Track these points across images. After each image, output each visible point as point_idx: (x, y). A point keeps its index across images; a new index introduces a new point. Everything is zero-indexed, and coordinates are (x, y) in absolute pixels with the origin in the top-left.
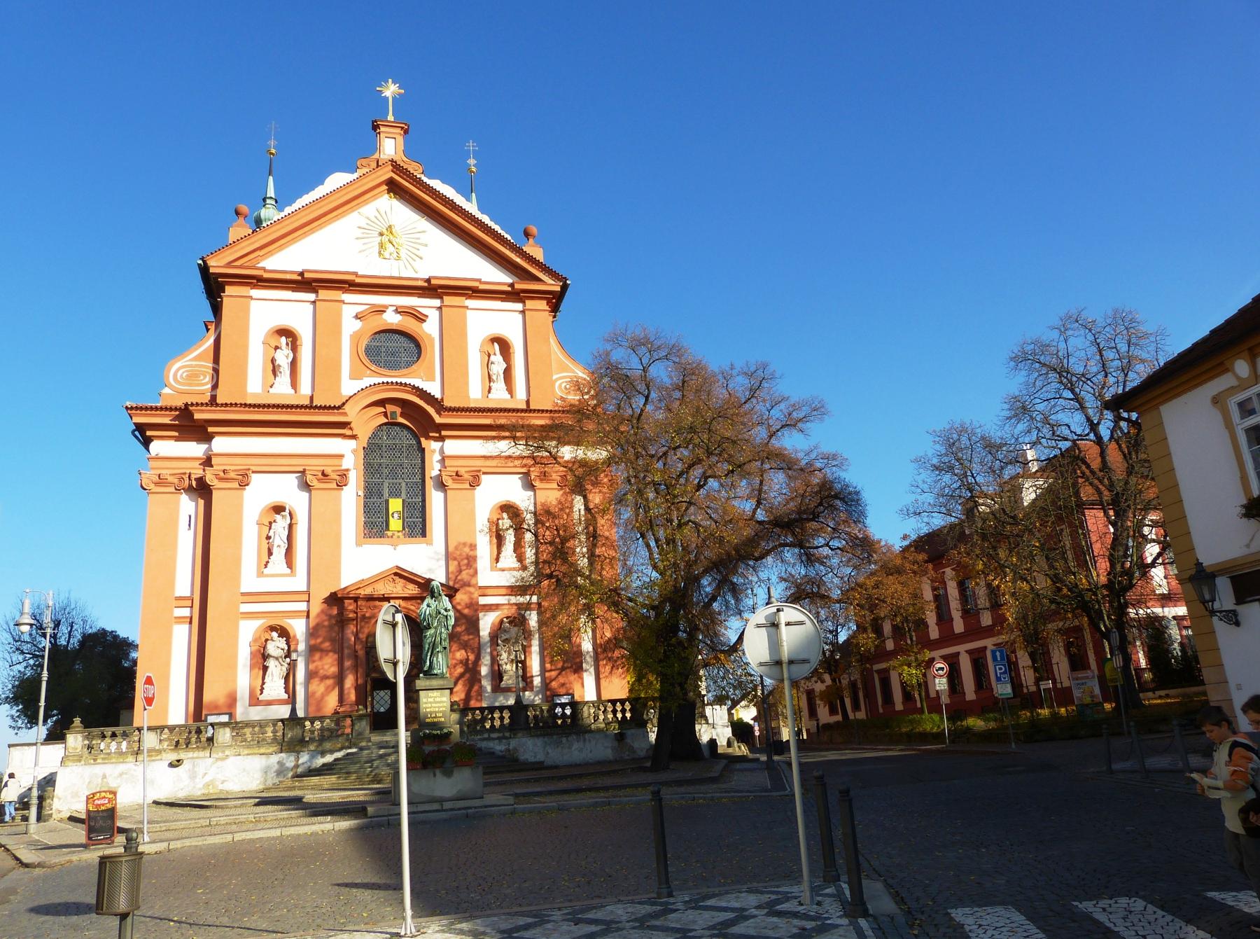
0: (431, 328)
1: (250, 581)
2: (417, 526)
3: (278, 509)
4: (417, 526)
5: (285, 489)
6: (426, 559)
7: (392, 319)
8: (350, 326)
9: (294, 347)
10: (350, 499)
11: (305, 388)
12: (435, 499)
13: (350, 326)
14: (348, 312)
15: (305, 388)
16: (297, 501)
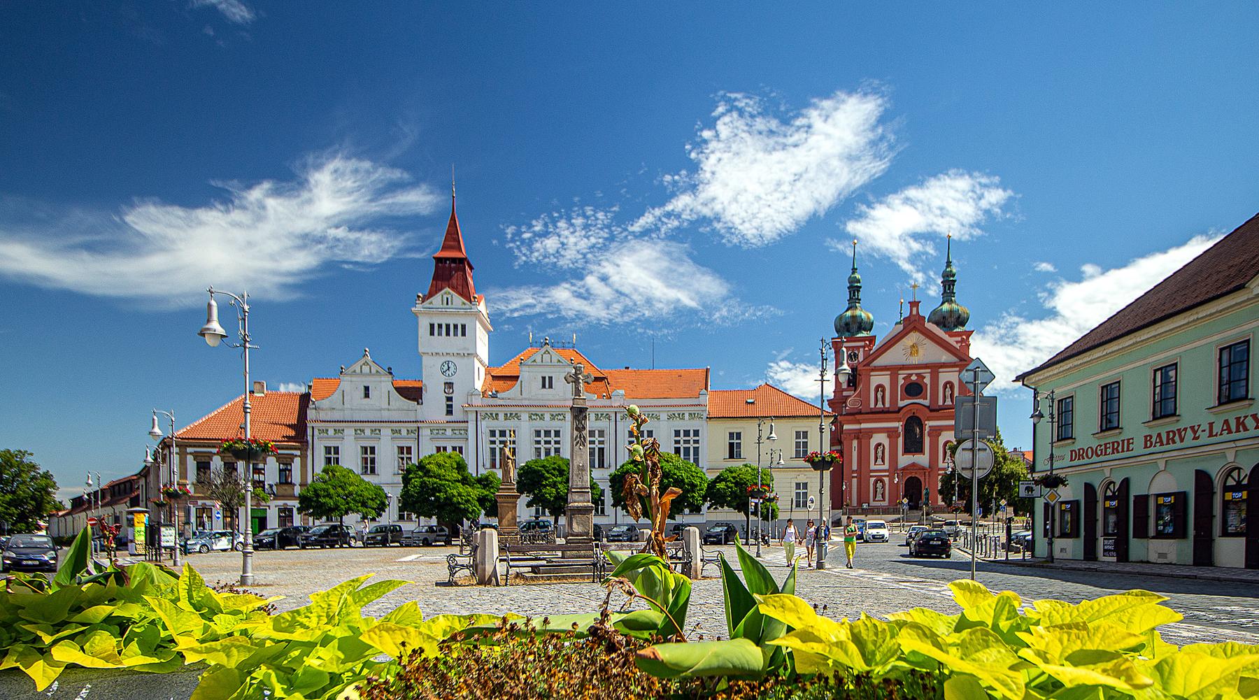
0: (927, 380)
1: (873, 467)
2: (921, 451)
3: (879, 445)
4: (921, 451)
5: (881, 438)
6: (923, 459)
7: (914, 378)
8: (901, 382)
9: (883, 391)
10: (900, 440)
11: (887, 405)
12: (927, 440)
13: (901, 382)
14: (901, 377)
15: (887, 405)
16: (886, 442)
